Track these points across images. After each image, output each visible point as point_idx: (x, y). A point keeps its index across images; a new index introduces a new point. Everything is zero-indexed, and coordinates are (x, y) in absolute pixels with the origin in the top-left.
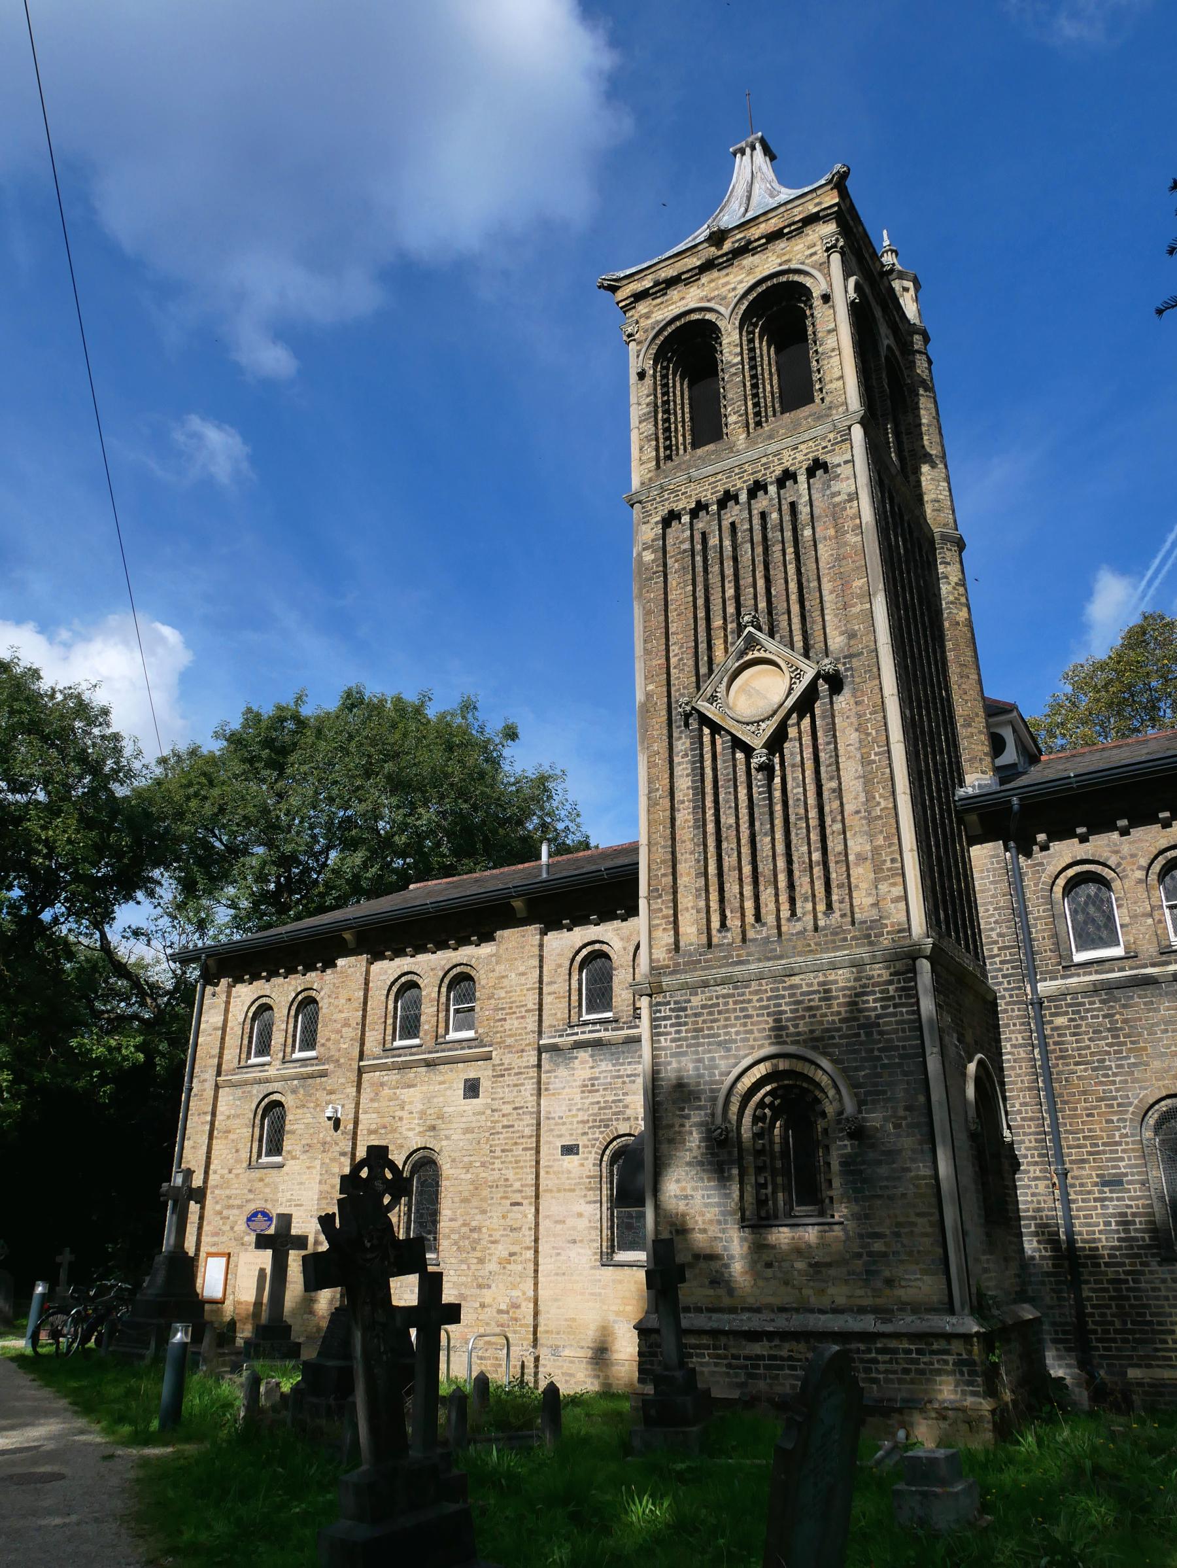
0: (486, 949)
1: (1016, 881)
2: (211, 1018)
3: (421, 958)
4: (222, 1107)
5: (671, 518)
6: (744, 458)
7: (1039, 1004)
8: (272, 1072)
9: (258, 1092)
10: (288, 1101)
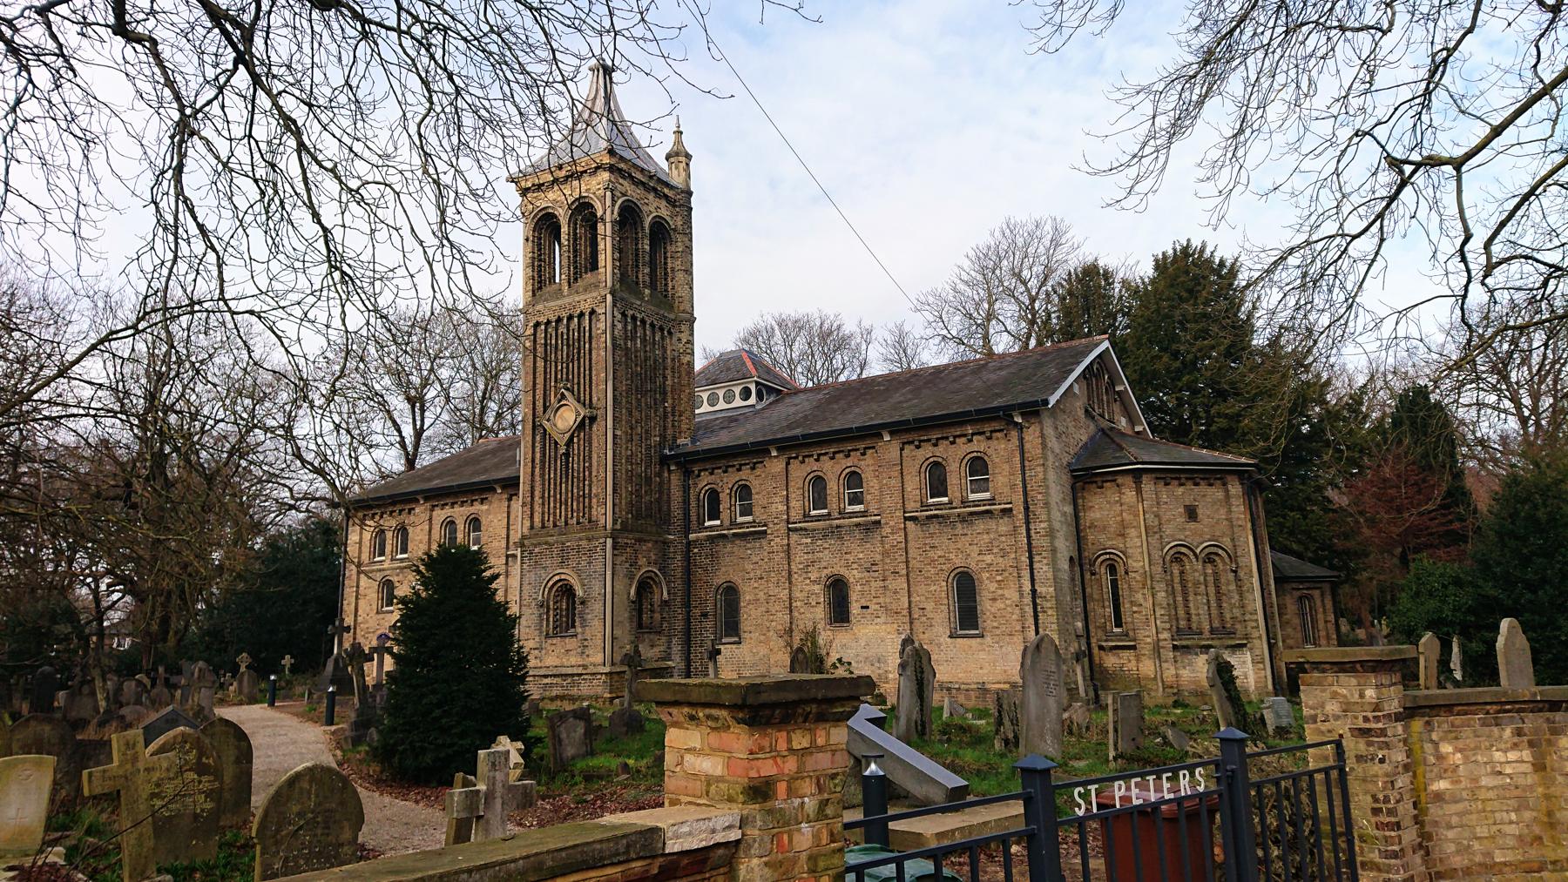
0: (485, 507)
1: (686, 490)
2: (353, 537)
3: (457, 509)
4: (362, 583)
5: (537, 325)
6: (567, 300)
7: (689, 543)
8: (386, 565)
9: (379, 576)
10: (395, 579)
